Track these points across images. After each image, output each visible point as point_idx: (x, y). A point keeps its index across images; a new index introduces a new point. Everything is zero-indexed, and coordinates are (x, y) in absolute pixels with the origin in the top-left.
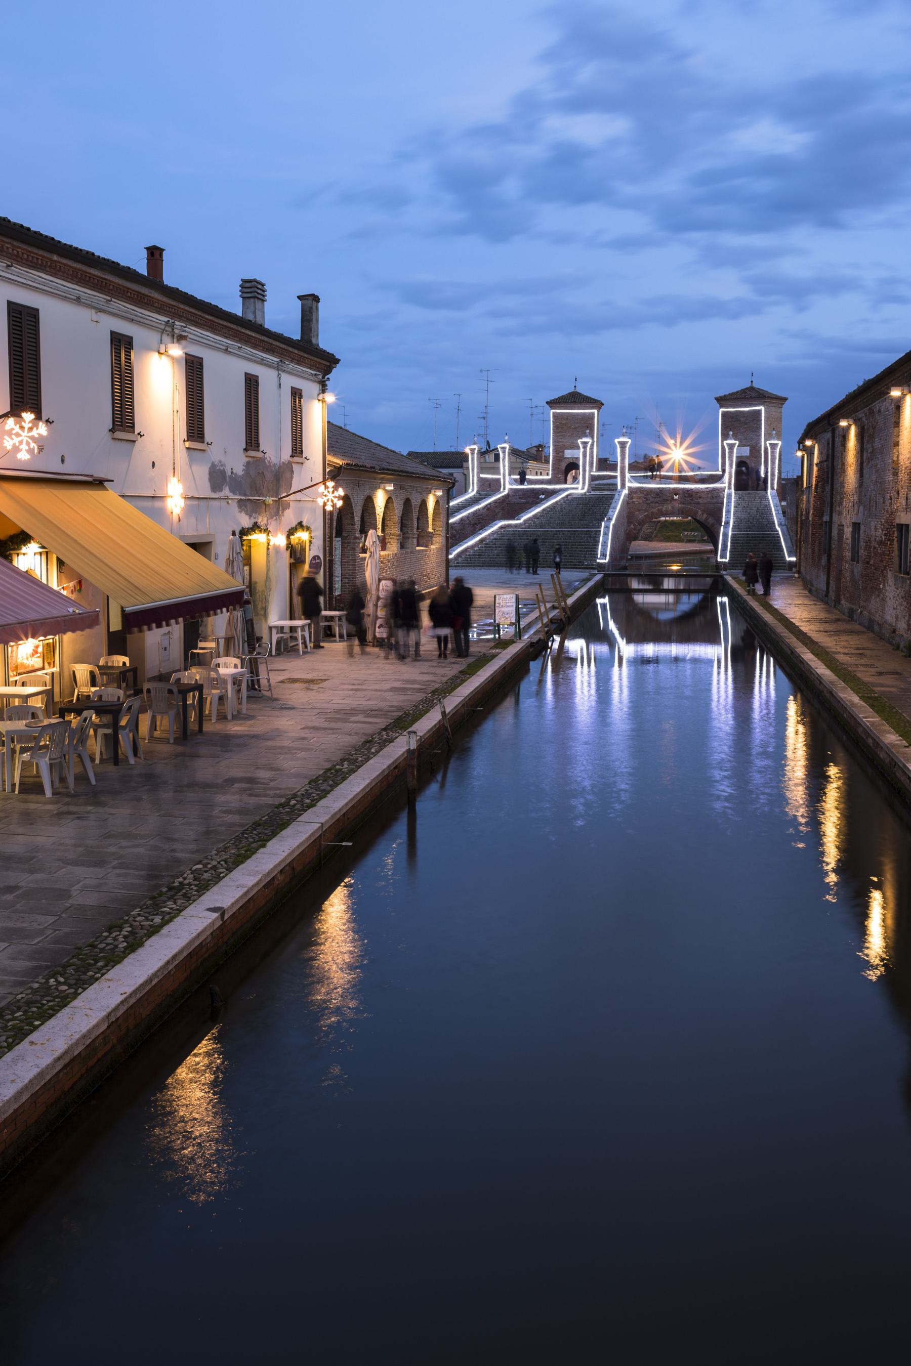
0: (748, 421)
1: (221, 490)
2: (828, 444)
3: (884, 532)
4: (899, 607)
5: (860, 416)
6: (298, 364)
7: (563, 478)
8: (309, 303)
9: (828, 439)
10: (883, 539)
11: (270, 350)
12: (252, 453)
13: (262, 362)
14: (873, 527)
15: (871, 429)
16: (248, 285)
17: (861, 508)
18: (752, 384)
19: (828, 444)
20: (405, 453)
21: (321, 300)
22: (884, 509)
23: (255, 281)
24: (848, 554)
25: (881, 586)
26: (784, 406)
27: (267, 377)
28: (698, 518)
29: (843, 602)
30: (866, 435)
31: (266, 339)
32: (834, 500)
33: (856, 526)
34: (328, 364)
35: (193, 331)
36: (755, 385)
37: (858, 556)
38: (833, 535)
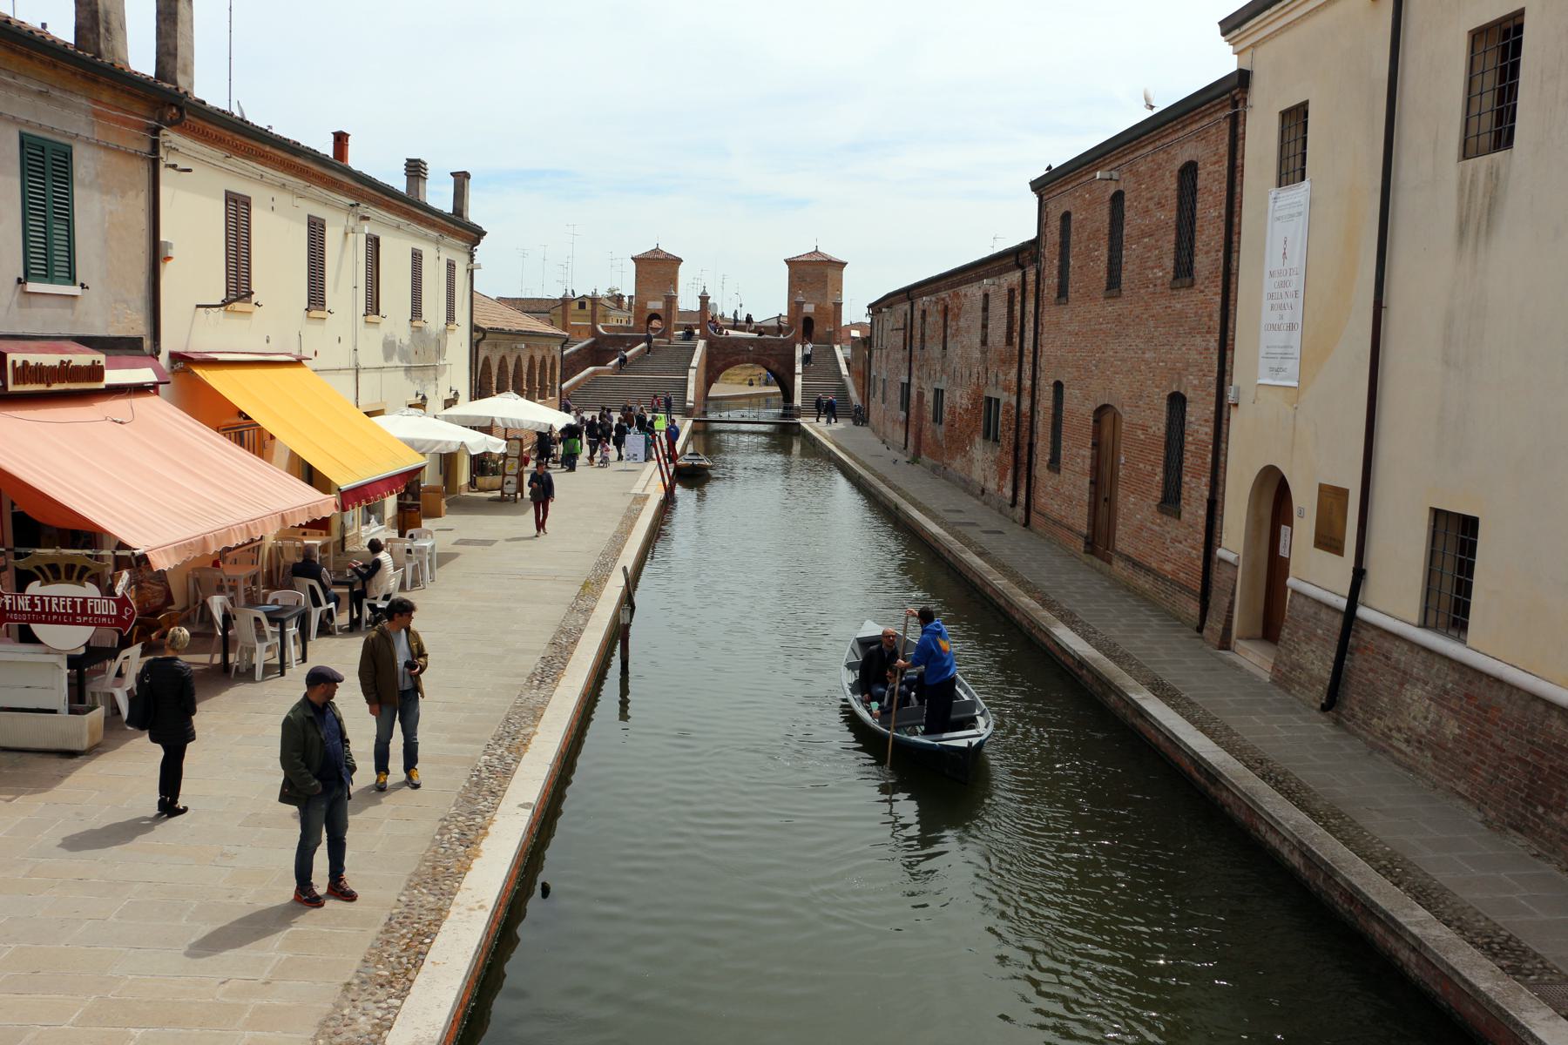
1: (392, 360)
2: (906, 315)
5: (944, 296)
6: (453, 237)
8: (461, 179)
11: (431, 225)
12: (416, 323)
13: (425, 238)
14: (958, 395)
15: (956, 310)
16: (413, 164)
17: (944, 377)
19: (906, 315)
20: (494, 298)
23: (419, 160)
24: (930, 416)
25: (968, 448)
27: (428, 252)
29: (923, 456)
31: (430, 216)
33: (939, 393)
34: (476, 236)
35: (372, 212)
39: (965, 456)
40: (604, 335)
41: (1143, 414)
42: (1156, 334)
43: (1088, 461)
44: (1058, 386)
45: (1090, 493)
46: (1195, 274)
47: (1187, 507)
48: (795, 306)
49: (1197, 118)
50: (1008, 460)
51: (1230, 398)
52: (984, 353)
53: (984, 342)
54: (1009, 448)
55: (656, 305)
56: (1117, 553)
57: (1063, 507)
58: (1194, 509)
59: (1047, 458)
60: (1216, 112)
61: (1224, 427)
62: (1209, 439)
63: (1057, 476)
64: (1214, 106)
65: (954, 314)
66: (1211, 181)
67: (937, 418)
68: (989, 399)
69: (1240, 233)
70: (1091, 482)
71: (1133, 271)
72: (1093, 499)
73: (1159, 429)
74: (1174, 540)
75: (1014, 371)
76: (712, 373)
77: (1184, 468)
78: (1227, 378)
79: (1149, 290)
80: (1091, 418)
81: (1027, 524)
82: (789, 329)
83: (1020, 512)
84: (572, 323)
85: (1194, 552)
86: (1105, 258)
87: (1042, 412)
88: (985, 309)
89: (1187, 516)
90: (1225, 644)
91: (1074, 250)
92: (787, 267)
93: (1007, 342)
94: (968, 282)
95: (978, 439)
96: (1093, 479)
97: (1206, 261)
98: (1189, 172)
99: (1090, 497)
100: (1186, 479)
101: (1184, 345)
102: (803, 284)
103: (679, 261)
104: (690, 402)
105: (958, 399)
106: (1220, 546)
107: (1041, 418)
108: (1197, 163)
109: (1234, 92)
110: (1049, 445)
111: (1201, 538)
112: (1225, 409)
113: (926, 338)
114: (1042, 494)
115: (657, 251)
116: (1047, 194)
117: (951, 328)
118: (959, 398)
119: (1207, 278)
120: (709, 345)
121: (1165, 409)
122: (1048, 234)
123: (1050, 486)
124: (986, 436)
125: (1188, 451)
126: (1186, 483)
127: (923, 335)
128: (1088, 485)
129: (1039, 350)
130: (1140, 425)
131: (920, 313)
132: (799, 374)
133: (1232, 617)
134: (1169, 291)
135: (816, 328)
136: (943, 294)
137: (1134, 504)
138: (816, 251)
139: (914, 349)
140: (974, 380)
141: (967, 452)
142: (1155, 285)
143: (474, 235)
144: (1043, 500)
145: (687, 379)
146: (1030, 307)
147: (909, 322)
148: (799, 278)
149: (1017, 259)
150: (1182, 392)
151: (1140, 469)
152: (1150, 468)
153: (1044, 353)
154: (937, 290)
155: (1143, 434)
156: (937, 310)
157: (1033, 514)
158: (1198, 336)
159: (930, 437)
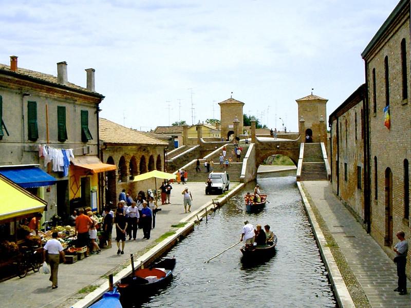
8: (90, 73)
27: (69, 108)
36: (313, 94)
40: (204, 143)
44: (376, 158)
48: (301, 123)
52: (356, 143)
55: (231, 127)
67: (346, 179)
70: (386, 209)
72: (387, 218)
81: (369, 231)
86: (385, 91)
92: (297, 103)
95: (356, 188)
96: (387, 207)
99: (386, 216)
102: (306, 112)
103: (243, 104)
115: (231, 99)
120: (256, 146)
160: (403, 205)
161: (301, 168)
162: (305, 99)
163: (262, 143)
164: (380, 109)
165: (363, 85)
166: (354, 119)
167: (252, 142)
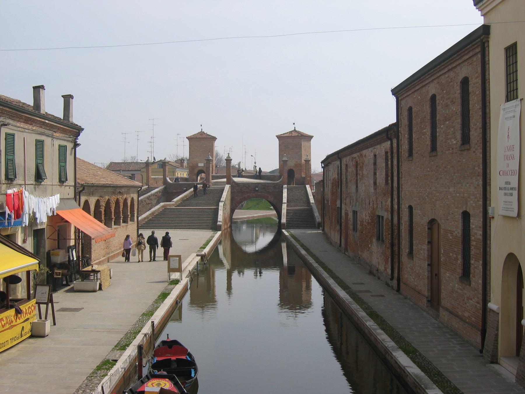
0: (293, 148)
2: (338, 167)
3: (370, 218)
4: (379, 258)
7: (196, 178)
8: (68, 99)
9: (338, 165)
10: (370, 221)
14: (364, 215)
17: (357, 203)
18: (295, 128)
21: (74, 98)
22: (370, 206)
24: (351, 227)
25: (370, 246)
26: (312, 140)
28: (269, 200)
29: (349, 251)
30: (359, 167)
32: (342, 197)
33: (355, 213)
36: (297, 129)
37: (357, 229)
38: (342, 215)
39: (369, 250)
41: (450, 224)
42: (454, 177)
43: (426, 252)
44: (411, 208)
45: (428, 271)
46: (471, 143)
47: (474, 279)
48: (283, 163)
49: (466, 52)
50: (389, 252)
51: (490, 214)
52: (375, 189)
53: (375, 183)
54: (388, 245)
56: (443, 307)
57: (416, 280)
58: (477, 280)
59: (407, 251)
60: (475, 49)
61: (488, 231)
62: (481, 238)
63: (412, 261)
64: (473, 45)
65: (361, 167)
66: (475, 87)
67: (355, 229)
68: (379, 216)
69: (490, 118)
70: (428, 265)
71: (442, 141)
73: (458, 233)
74: (468, 298)
75: (390, 200)
76: (235, 204)
77: (471, 256)
78: (488, 202)
79: (450, 151)
80: (427, 227)
81: (398, 290)
82: (280, 177)
83: (395, 282)
84: (152, 177)
85: (478, 305)
86: (429, 133)
87: (404, 224)
88: (375, 164)
89: (474, 284)
90: (495, 360)
91: (414, 130)
93: (385, 183)
94: (367, 148)
95: (374, 240)
96: (429, 263)
97: (475, 134)
98: (465, 82)
99: (428, 274)
100: (472, 262)
101: (468, 183)
104: (220, 222)
105: (364, 217)
106: (490, 301)
107: (403, 227)
108: (468, 78)
109: (482, 38)
110: (407, 243)
111: (480, 296)
112: (488, 220)
113: (348, 181)
114: (405, 272)
116: (400, 96)
117: (359, 175)
118: (364, 216)
119: (476, 144)
120: (232, 188)
121: (460, 221)
122: (402, 120)
123: (409, 268)
124: (378, 239)
125: (472, 245)
126: (473, 264)
127: (346, 179)
128: (426, 266)
129: (400, 188)
130: (449, 231)
131: (345, 166)
132: (285, 203)
133: (497, 344)
134: (460, 152)
135: (296, 176)
136: (355, 155)
137: (449, 277)
138: (295, 130)
139: (343, 187)
140: (371, 205)
141: (369, 248)
142: (453, 149)
143: (77, 131)
144: (406, 276)
145: (218, 208)
146: (395, 162)
147: (340, 171)
148: (285, 146)
149: (387, 135)
150: (468, 211)
151: (451, 256)
152: (455, 256)
153: (403, 189)
154: (352, 153)
155: (451, 236)
156: (353, 165)
157: (401, 284)
158: (474, 178)
159: (352, 239)
160: (460, 261)
161: (285, 213)
162: (287, 135)
163: (237, 184)
164: (419, 153)
165: (392, 126)
166: (372, 162)
167: (228, 183)
